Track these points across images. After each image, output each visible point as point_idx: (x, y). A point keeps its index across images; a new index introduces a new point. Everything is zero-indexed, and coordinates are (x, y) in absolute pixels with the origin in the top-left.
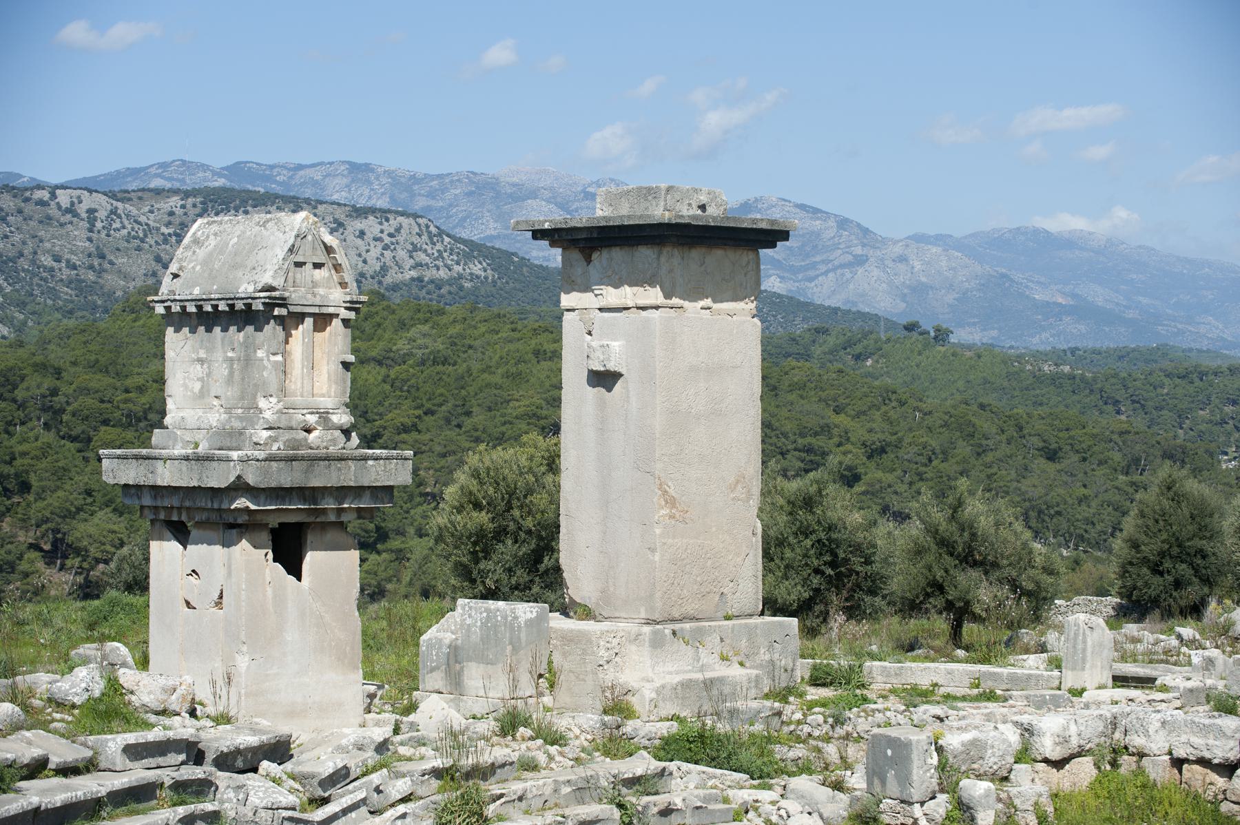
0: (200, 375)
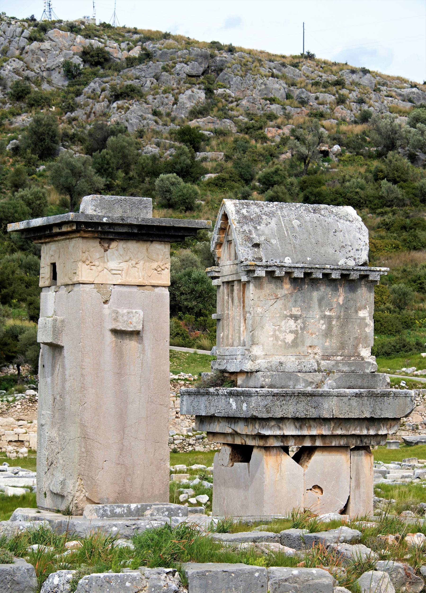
0: (294, 328)
